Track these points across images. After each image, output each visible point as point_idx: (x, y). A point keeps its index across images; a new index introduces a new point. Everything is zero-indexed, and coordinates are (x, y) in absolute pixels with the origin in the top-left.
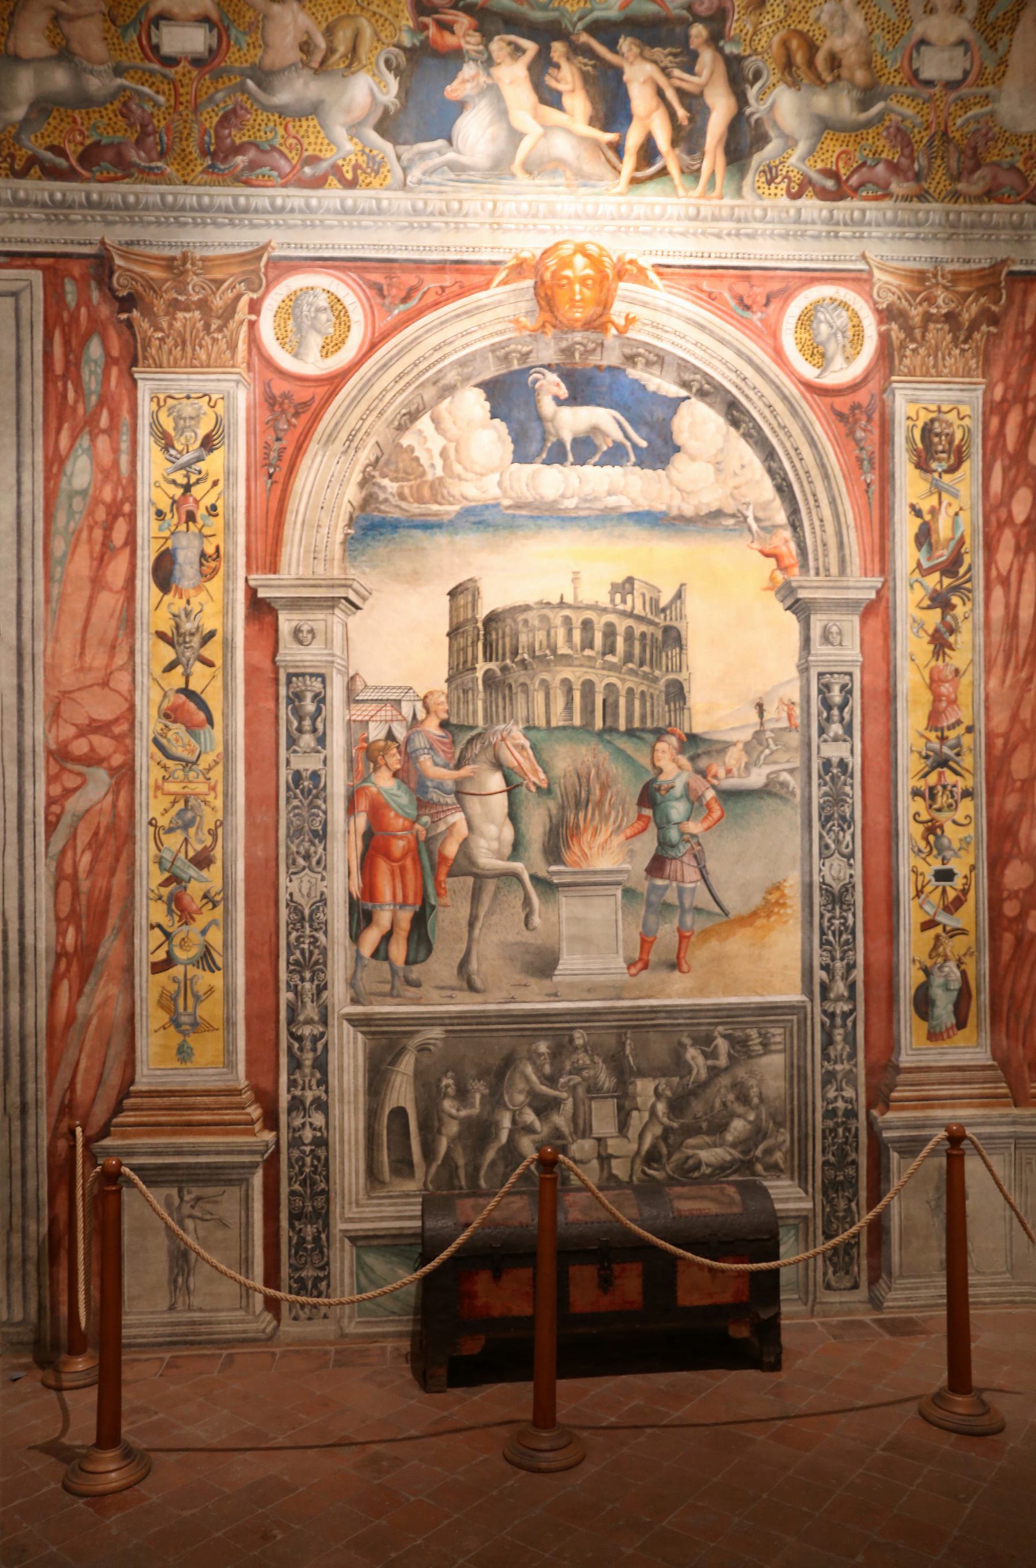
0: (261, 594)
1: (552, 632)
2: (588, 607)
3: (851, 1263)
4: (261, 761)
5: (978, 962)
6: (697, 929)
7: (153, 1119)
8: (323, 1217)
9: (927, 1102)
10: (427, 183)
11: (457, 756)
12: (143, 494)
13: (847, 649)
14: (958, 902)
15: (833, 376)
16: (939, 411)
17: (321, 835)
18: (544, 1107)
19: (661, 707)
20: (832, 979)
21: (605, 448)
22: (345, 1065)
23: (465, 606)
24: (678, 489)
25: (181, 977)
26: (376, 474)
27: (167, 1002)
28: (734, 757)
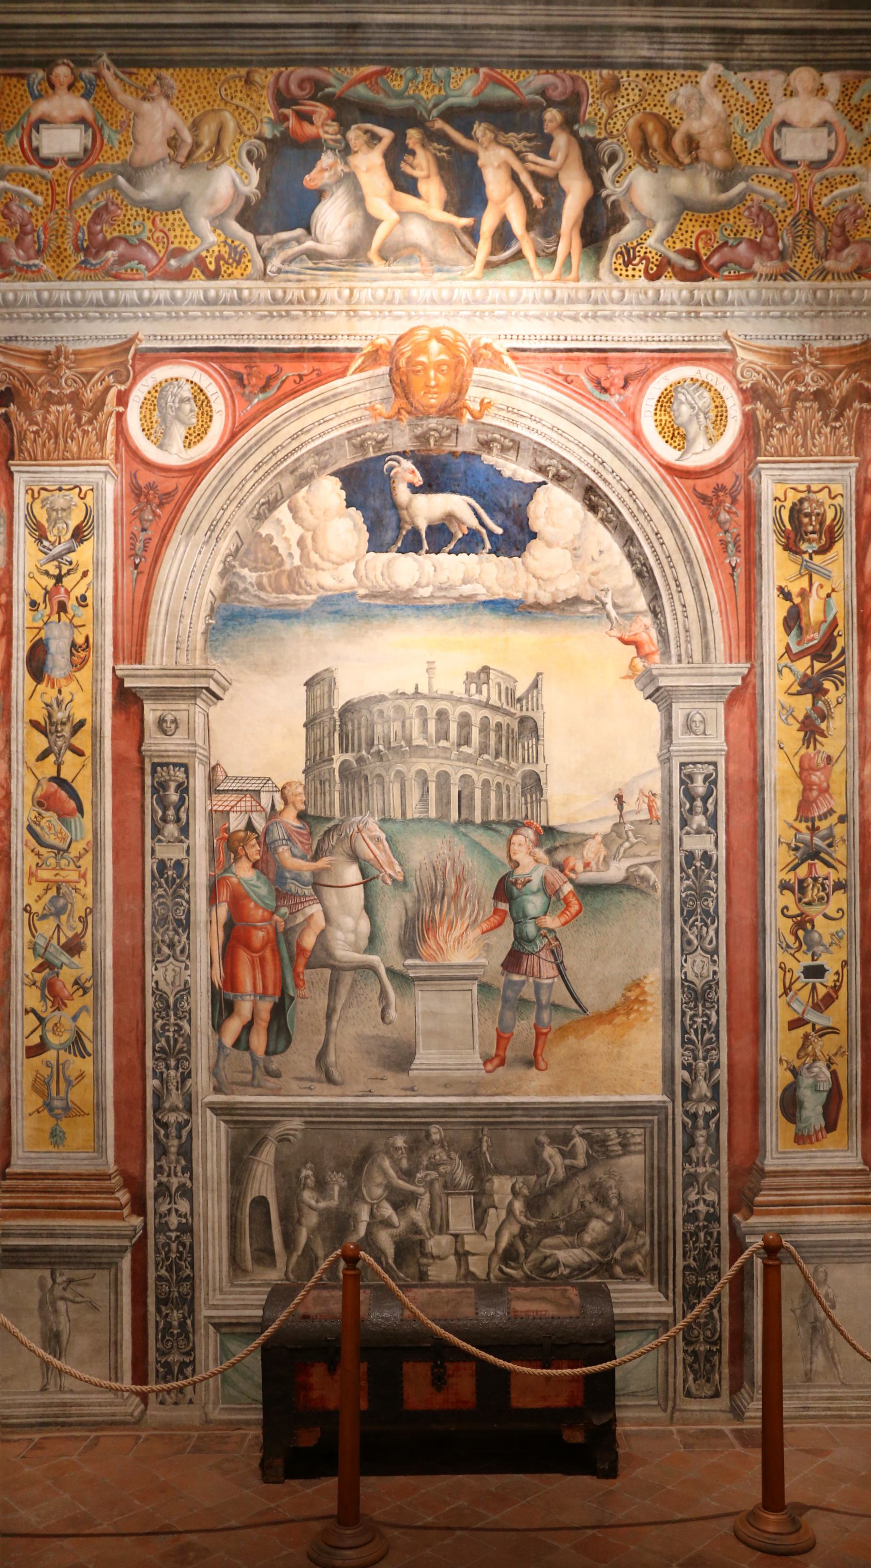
1: (407, 722)
2: (443, 698)
14: (829, 1000)
15: (694, 458)
16: (809, 490)
19: (517, 798)
21: (460, 536)
23: (322, 697)
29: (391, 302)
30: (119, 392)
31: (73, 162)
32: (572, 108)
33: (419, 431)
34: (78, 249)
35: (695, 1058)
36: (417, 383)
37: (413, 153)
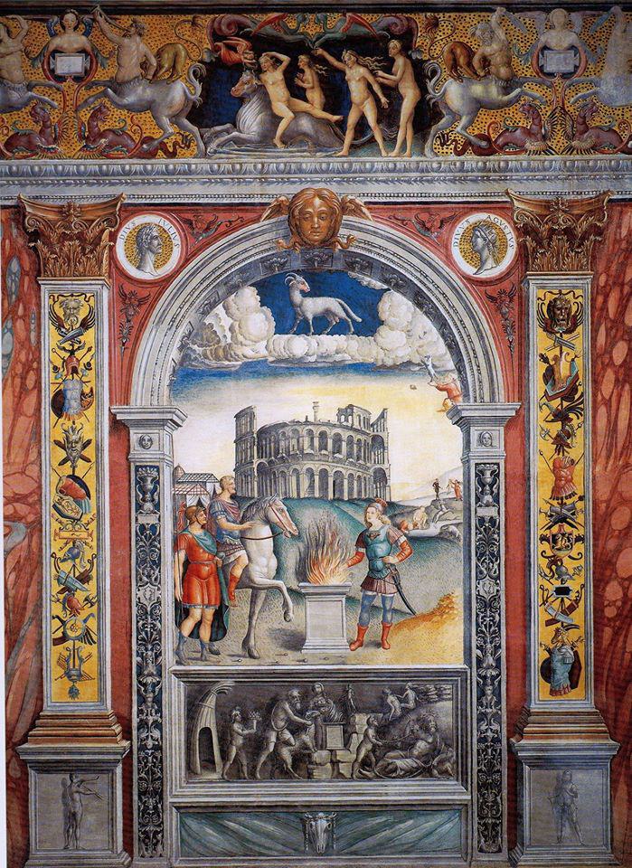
0: (118, 418)
2: (323, 424)
3: (497, 836)
4: (120, 520)
5: (586, 646)
7: (54, 732)
8: (159, 794)
9: (548, 734)
10: (220, 153)
12: (46, 356)
13: (496, 449)
14: (572, 608)
16: (560, 293)
17: (157, 564)
18: (297, 729)
22: (173, 701)
25: (71, 648)
27: (64, 662)
28: (419, 516)
29: (289, 173)
30: (111, 232)
31: (77, 79)
32: (407, 38)
34: (81, 137)
35: (485, 643)
36: (307, 225)
37: (303, 72)
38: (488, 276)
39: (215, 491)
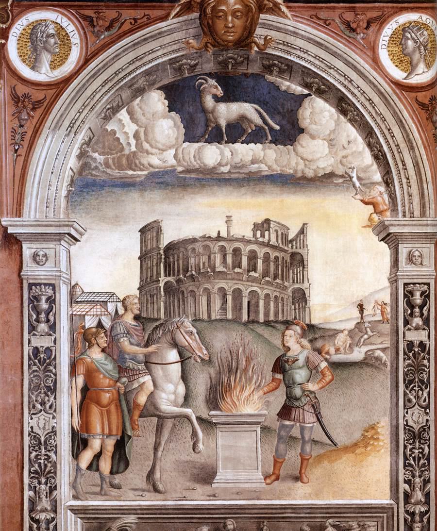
0: (9, 231)
1: (212, 256)
2: (237, 240)
6: (314, 454)
11: (146, 338)
17: (53, 390)
19: (289, 307)
20: (413, 490)
21: (250, 131)
24: (302, 158)
26: (89, 149)
28: (341, 340)
33: (221, 58)
35: (413, 476)
36: (220, 25)
38: (419, 82)
39: (117, 311)
